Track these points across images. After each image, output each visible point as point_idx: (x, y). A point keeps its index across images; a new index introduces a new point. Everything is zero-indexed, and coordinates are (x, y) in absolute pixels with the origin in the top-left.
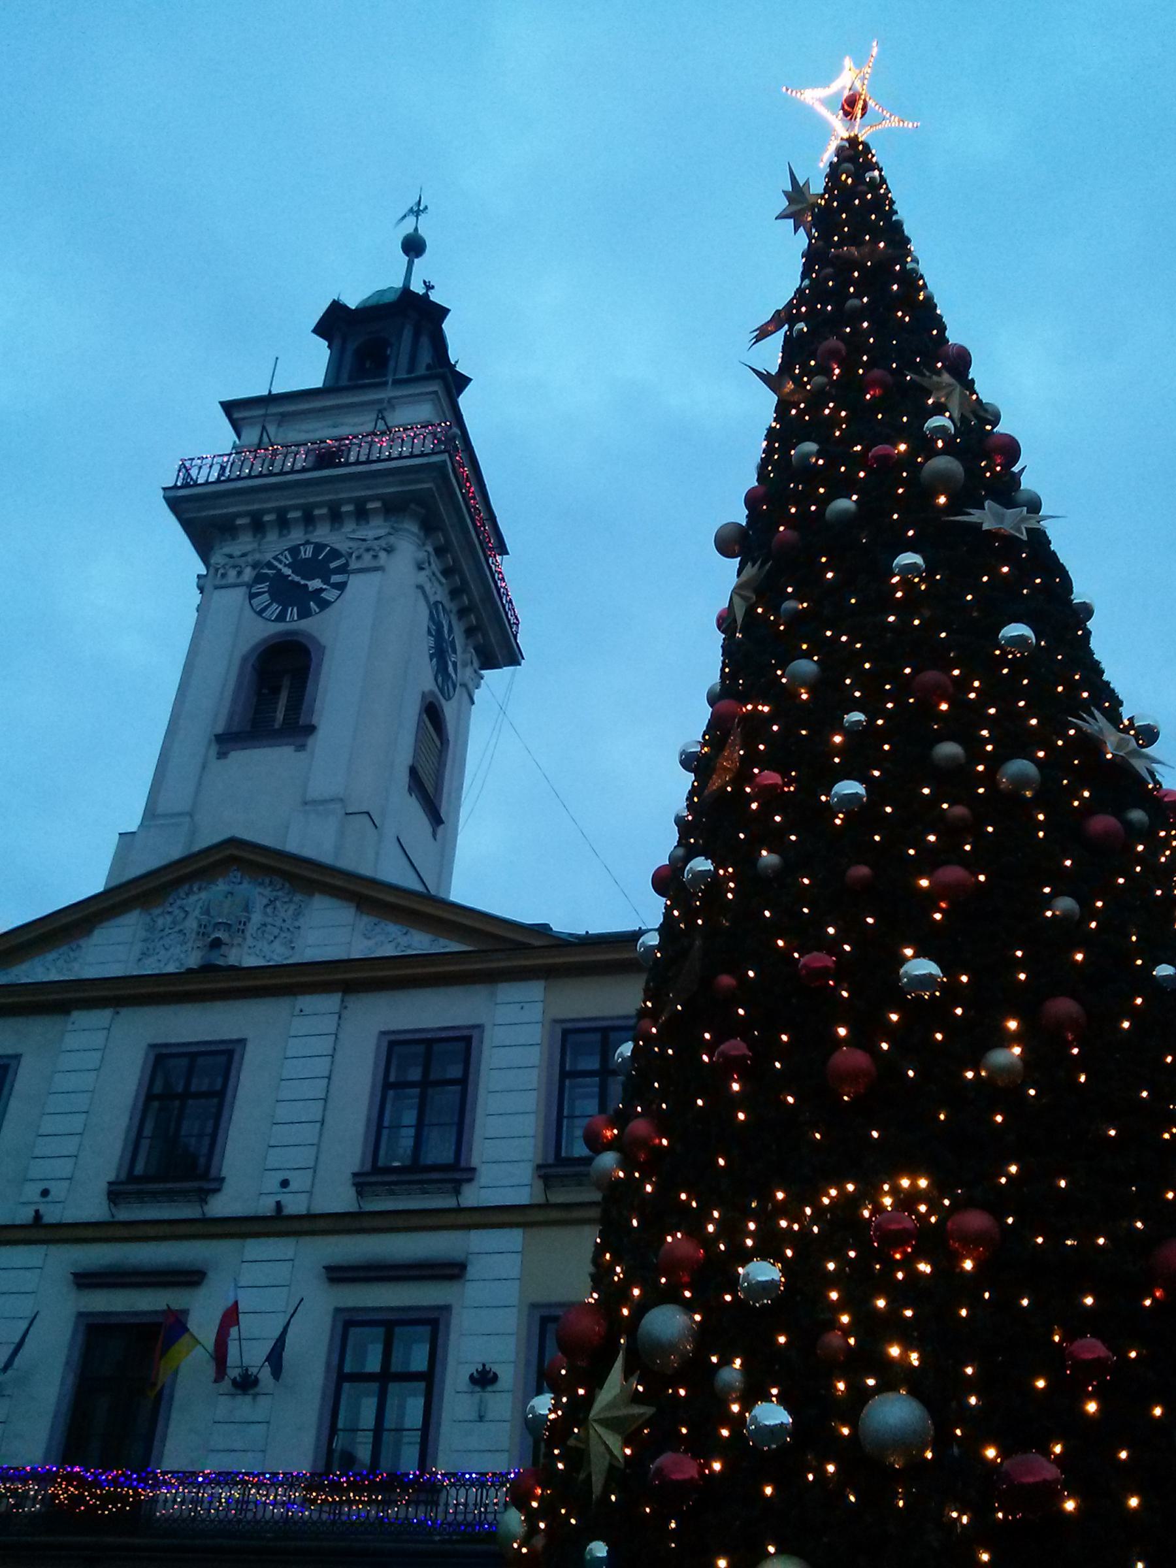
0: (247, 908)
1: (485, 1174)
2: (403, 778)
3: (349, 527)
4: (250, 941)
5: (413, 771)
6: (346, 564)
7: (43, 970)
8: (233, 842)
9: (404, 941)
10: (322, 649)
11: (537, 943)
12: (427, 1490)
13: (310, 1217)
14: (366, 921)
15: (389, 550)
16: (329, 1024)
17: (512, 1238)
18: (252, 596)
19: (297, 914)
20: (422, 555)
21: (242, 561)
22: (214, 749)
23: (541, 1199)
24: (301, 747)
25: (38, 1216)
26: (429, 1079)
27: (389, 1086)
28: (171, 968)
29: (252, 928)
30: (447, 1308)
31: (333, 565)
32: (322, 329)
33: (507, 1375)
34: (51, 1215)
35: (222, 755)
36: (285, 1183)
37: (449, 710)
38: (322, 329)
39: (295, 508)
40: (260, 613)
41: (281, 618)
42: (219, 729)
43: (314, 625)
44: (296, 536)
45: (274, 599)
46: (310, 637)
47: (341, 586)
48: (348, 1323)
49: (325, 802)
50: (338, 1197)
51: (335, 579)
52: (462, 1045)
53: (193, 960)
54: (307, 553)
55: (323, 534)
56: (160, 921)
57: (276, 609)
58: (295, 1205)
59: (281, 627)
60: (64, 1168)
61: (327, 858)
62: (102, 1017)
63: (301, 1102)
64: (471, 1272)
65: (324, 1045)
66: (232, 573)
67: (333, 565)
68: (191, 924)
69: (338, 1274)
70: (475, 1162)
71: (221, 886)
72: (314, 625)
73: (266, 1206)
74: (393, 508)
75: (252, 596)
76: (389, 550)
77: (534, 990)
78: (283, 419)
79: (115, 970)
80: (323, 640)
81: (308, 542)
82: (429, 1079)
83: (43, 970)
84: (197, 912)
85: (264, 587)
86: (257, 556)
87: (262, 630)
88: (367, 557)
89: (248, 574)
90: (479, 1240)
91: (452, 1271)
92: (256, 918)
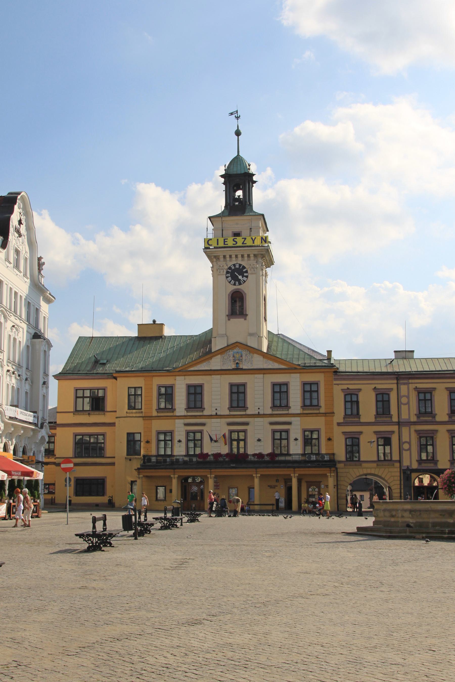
0: (241, 356)
1: (292, 408)
4: (243, 363)
8: (237, 342)
10: (245, 294)
11: (298, 367)
12: (288, 454)
13: (264, 414)
14: (265, 360)
17: (298, 419)
18: (227, 277)
19: (252, 357)
22: (227, 318)
23: (302, 412)
24: (245, 319)
28: (230, 368)
29: (243, 360)
30: (289, 429)
31: (244, 270)
34: (218, 414)
35: (229, 320)
36: (259, 409)
40: (230, 282)
42: (227, 314)
45: (232, 279)
47: (247, 277)
48: (274, 432)
50: (269, 411)
51: (245, 274)
52: (286, 384)
53: (234, 366)
54: (237, 266)
56: (225, 357)
57: (233, 282)
58: (261, 412)
59: (235, 287)
63: (259, 394)
64: (292, 424)
66: (222, 271)
67: (244, 270)
68: (231, 358)
70: (290, 406)
73: (256, 412)
75: (227, 277)
77: (298, 375)
79: (219, 368)
80: (246, 292)
81: (237, 263)
84: (232, 356)
85: (229, 275)
91: (289, 423)
92: (244, 357)
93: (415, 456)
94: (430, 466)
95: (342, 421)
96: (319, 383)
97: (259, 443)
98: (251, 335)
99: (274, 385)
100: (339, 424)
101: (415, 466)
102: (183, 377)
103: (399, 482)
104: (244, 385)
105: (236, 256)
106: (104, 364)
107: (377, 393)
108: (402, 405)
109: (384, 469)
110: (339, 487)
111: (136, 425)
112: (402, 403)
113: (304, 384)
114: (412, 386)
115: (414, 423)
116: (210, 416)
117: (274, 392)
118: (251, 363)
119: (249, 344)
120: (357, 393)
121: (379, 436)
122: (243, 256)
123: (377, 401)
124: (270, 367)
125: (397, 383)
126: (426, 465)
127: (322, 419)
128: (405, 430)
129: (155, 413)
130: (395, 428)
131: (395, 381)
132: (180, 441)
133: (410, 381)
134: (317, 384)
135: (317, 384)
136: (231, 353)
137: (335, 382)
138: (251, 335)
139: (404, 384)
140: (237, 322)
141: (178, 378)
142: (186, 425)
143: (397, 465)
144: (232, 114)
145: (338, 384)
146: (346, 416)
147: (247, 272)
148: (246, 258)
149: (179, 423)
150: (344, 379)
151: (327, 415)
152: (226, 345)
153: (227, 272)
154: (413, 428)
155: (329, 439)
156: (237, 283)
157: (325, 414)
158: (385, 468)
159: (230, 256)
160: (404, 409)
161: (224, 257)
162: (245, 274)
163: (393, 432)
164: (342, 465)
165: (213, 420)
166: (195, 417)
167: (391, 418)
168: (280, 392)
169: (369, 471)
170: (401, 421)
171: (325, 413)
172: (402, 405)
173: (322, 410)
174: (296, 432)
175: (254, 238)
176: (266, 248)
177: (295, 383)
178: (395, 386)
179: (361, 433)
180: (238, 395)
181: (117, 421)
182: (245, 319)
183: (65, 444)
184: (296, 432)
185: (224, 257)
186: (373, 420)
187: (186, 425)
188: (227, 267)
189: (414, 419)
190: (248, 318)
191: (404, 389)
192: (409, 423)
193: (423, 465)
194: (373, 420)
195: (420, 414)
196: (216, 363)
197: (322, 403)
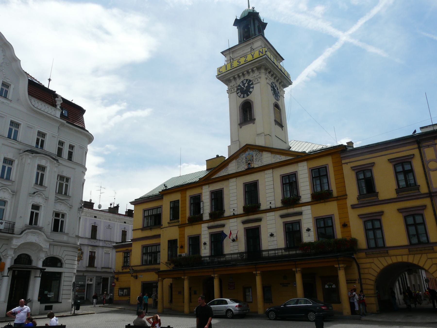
0: (252, 157)
2: (273, 123)
3: (251, 74)
5: (275, 121)
6: (253, 83)
7: (223, 173)
8: (247, 145)
9: (280, 158)
11: (303, 155)
13: (276, 208)
14: (273, 155)
17: (309, 207)
18: (237, 93)
19: (261, 156)
20: (266, 76)
21: (233, 87)
22: (239, 126)
24: (254, 123)
25: (234, 214)
27: (284, 184)
28: (243, 169)
29: (254, 160)
30: (300, 220)
32: (235, 24)
34: (236, 213)
35: (241, 127)
36: (270, 203)
37: (279, 103)
38: (235, 24)
39: (240, 73)
40: (240, 97)
41: (244, 97)
43: (251, 97)
44: (242, 79)
46: (250, 100)
47: (253, 88)
49: (261, 134)
51: (251, 86)
52: (295, 174)
53: (246, 167)
55: (247, 77)
58: (273, 206)
60: (236, 205)
61: (264, 145)
62: (234, 180)
65: (271, 179)
66: (233, 90)
68: (244, 161)
69: (282, 216)
71: (247, 153)
72: (251, 97)
73: (268, 207)
74: (259, 68)
75: (237, 93)
76: (260, 78)
78: (233, 52)
80: (253, 100)
83: (223, 173)
85: (239, 91)
86: (236, 85)
87: (241, 100)
88: (256, 80)
89: (236, 89)
90: (303, 209)
91: (300, 214)
92: (254, 158)
96: (327, 166)
97: (272, 238)
98: (258, 135)
99: (283, 177)
100: (354, 207)
105: (243, 75)
107: (394, 163)
108: (431, 173)
109: (419, 256)
110: (363, 281)
112: (430, 170)
113: (312, 170)
117: (283, 184)
118: (261, 161)
120: (370, 168)
121: (405, 214)
122: (248, 73)
123: (397, 173)
124: (278, 160)
125: (419, 148)
130: (427, 202)
131: (416, 146)
134: (325, 168)
135: (325, 168)
136: (244, 156)
137: (343, 162)
139: (428, 146)
140: (249, 127)
145: (347, 163)
149: (204, 227)
150: (353, 156)
151: (339, 198)
152: (238, 149)
153: (238, 89)
155: (345, 225)
157: (337, 199)
158: (422, 254)
159: (239, 76)
162: (251, 86)
163: (424, 207)
164: (363, 255)
168: (290, 183)
169: (400, 259)
171: (337, 197)
172: (431, 173)
175: (253, 54)
176: (264, 57)
177: (303, 172)
178: (416, 152)
182: (254, 123)
187: (209, 228)
190: (257, 121)
191: (429, 153)
197: (333, 187)
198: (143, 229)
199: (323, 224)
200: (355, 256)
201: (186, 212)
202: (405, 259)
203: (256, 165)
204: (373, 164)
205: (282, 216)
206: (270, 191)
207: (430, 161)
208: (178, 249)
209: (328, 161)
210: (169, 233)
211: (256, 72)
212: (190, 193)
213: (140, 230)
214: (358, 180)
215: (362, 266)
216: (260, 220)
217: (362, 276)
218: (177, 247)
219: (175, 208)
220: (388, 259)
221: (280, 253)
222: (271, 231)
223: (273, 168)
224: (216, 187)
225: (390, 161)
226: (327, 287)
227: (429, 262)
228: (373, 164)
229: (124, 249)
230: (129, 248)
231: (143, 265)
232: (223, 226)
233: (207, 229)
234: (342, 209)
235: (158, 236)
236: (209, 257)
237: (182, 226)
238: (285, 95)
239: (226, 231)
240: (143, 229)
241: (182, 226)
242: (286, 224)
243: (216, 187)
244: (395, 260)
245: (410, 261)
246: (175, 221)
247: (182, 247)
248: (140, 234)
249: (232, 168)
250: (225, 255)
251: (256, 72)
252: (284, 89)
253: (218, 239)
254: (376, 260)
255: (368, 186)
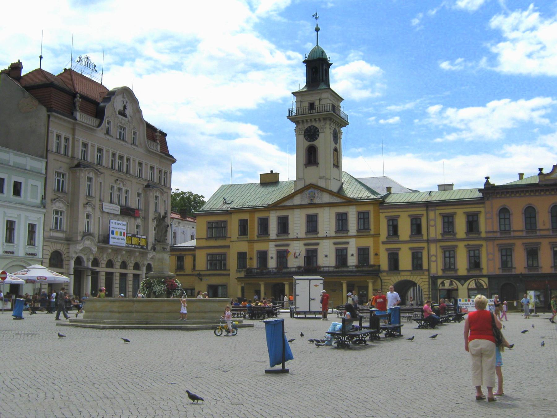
1: (351, 231)
7: (289, 203)
8: (311, 184)
14: (331, 196)
15: (325, 128)
16: (328, 211)
17: (354, 239)
18: (305, 136)
26: (342, 220)
28: (306, 203)
32: (304, 62)
33: (355, 255)
34: (299, 237)
35: (306, 167)
37: (337, 146)
43: (315, 143)
47: (319, 135)
50: (333, 234)
52: (346, 214)
53: (309, 202)
58: (328, 235)
61: (324, 187)
68: (307, 196)
69: (335, 244)
71: (310, 190)
73: (325, 235)
74: (325, 119)
78: (302, 95)
82: (342, 220)
83: (289, 203)
87: (307, 144)
91: (348, 243)
92: (316, 195)
93: (440, 265)
94: (452, 273)
95: (385, 240)
97: (326, 258)
98: (321, 178)
100: (383, 243)
101: (440, 273)
102: (275, 212)
103: (427, 286)
104: (316, 216)
105: (311, 120)
106: (229, 204)
111: (243, 247)
113: (359, 213)
114: (438, 212)
115: (439, 241)
116: (293, 240)
119: (319, 185)
121: (413, 251)
122: (315, 120)
124: (335, 201)
125: (427, 210)
126: (449, 272)
127: (371, 239)
128: (433, 247)
129: (256, 238)
130: (425, 245)
131: (425, 209)
132: (272, 258)
133: (438, 208)
134: (368, 213)
135: (368, 213)
136: (307, 192)
137: (381, 211)
138: (321, 178)
139: (432, 210)
140: (312, 169)
141: (271, 212)
142: (276, 246)
143: (427, 273)
144: (314, 16)
146: (389, 236)
147: (318, 131)
148: (318, 122)
149: (272, 244)
153: (305, 132)
154: (439, 244)
155: (376, 254)
156: (312, 140)
159: (307, 120)
160: (432, 230)
161: (303, 121)
163: (423, 248)
164: (385, 274)
165: (295, 242)
166: (282, 240)
167: (422, 237)
169: (405, 278)
170: (430, 239)
173: (372, 232)
174: (352, 249)
177: (352, 213)
178: (424, 213)
179: (400, 249)
180: (312, 223)
181: (231, 244)
183: (202, 263)
184: (352, 249)
185: (303, 121)
186: (408, 239)
187: (276, 246)
188: (304, 129)
189: (440, 237)
190: (320, 165)
191: (432, 215)
192: (436, 241)
193: (446, 272)
194: (408, 239)
195: (444, 233)
196: (297, 201)
197: (372, 227)
198: (208, 238)
199: (363, 253)
200: (380, 275)
201: (254, 229)
202: (408, 278)
203: (317, 201)
204: (399, 216)
205: (335, 244)
206: (327, 222)
207: (432, 220)
208: (247, 260)
209: (370, 208)
210: (237, 246)
211: (322, 121)
212: (258, 215)
213: (204, 240)
214: (388, 225)
215: (383, 281)
216: (317, 244)
217: (384, 287)
218: (246, 258)
219: (243, 227)
220: (399, 277)
221: (331, 269)
222: (326, 253)
223: (330, 206)
224: (283, 213)
225: (409, 216)
226: (361, 293)
227: (421, 280)
228: (399, 216)
229: (178, 253)
230: (183, 253)
231: (208, 270)
232: (288, 245)
233: (273, 246)
234: (376, 244)
235: (228, 247)
236: (276, 268)
237: (251, 242)
238: (343, 137)
239: (290, 249)
240: (208, 238)
241: (251, 242)
242: (337, 250)
243: (283, 213)
244: (403, 278)
245: (411, 279)
246: (245, 236)
247: (251, 259)
248: (204, 243)
249: (297, 201)
250: (288, 268)
251: (322, 121)
252: (343, 129)
253: (282, 256)
254: (392, 278)
255: (394, 229)
